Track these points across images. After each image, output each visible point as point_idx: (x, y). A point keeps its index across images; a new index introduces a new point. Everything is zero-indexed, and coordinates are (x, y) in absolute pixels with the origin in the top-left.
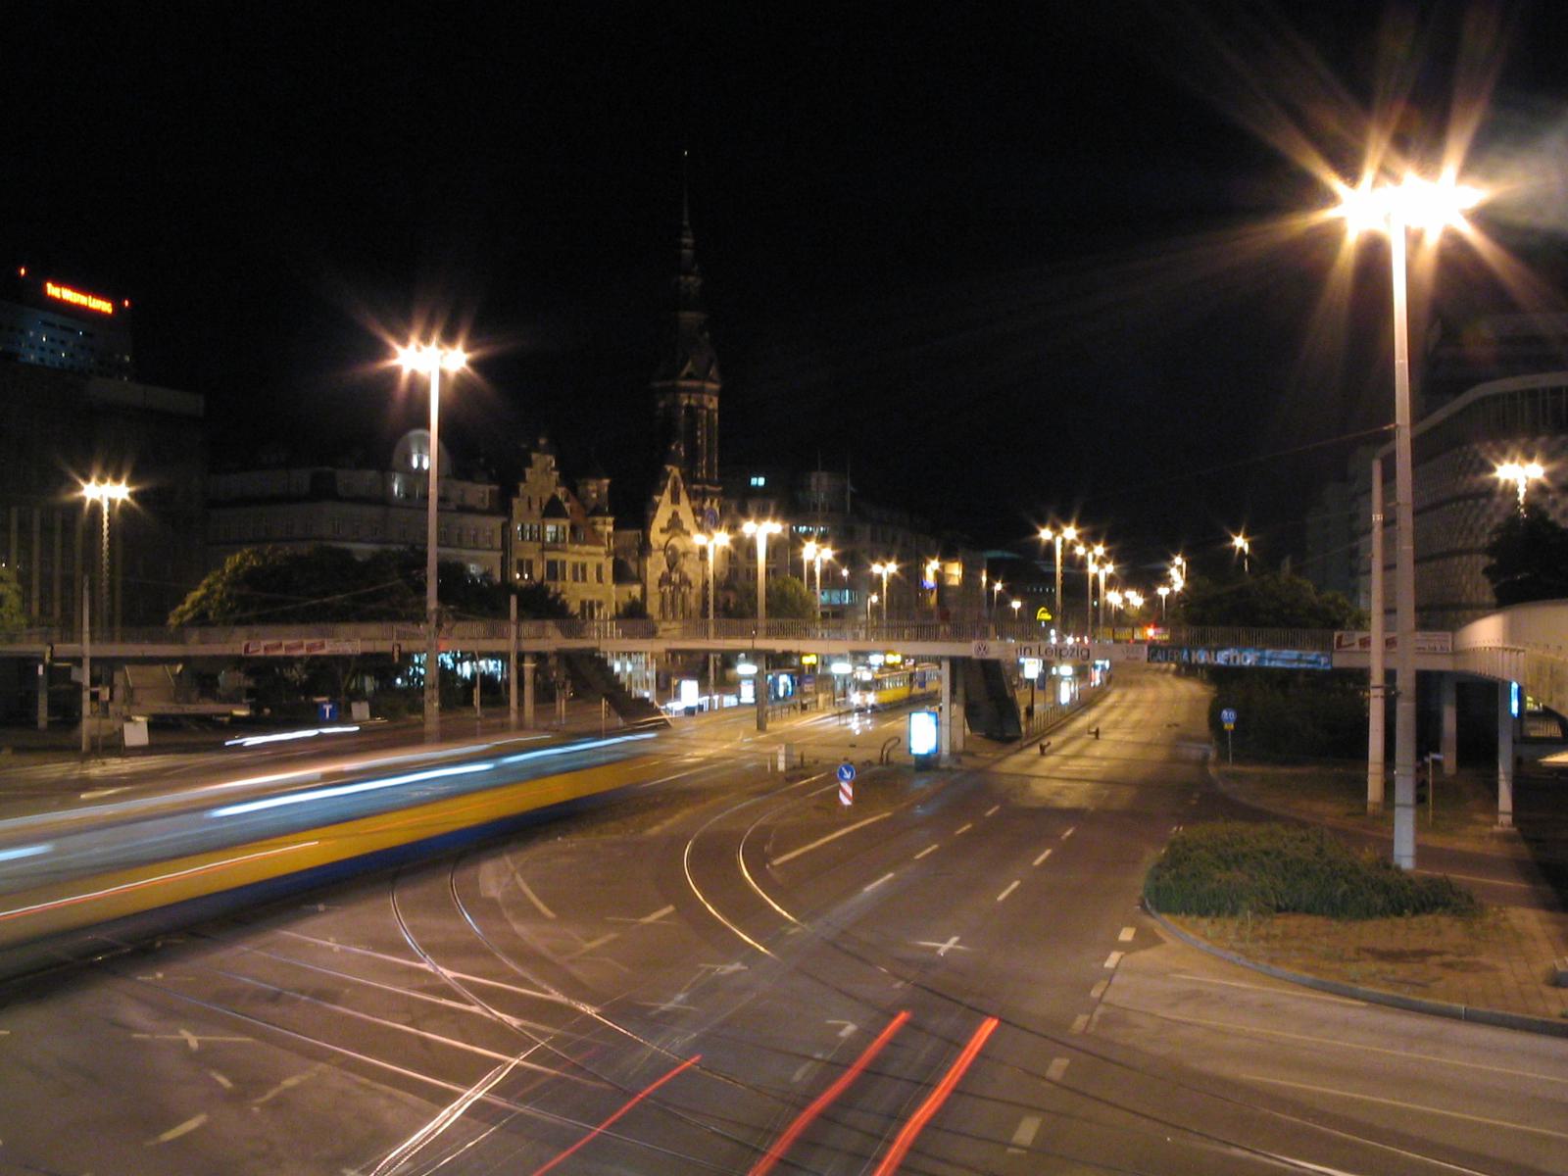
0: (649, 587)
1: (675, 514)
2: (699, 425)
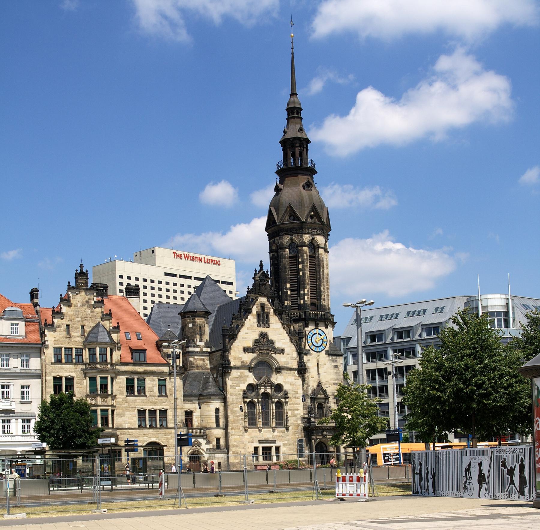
0: (230, 399)
1: (264, 336)
2: (300, 260)
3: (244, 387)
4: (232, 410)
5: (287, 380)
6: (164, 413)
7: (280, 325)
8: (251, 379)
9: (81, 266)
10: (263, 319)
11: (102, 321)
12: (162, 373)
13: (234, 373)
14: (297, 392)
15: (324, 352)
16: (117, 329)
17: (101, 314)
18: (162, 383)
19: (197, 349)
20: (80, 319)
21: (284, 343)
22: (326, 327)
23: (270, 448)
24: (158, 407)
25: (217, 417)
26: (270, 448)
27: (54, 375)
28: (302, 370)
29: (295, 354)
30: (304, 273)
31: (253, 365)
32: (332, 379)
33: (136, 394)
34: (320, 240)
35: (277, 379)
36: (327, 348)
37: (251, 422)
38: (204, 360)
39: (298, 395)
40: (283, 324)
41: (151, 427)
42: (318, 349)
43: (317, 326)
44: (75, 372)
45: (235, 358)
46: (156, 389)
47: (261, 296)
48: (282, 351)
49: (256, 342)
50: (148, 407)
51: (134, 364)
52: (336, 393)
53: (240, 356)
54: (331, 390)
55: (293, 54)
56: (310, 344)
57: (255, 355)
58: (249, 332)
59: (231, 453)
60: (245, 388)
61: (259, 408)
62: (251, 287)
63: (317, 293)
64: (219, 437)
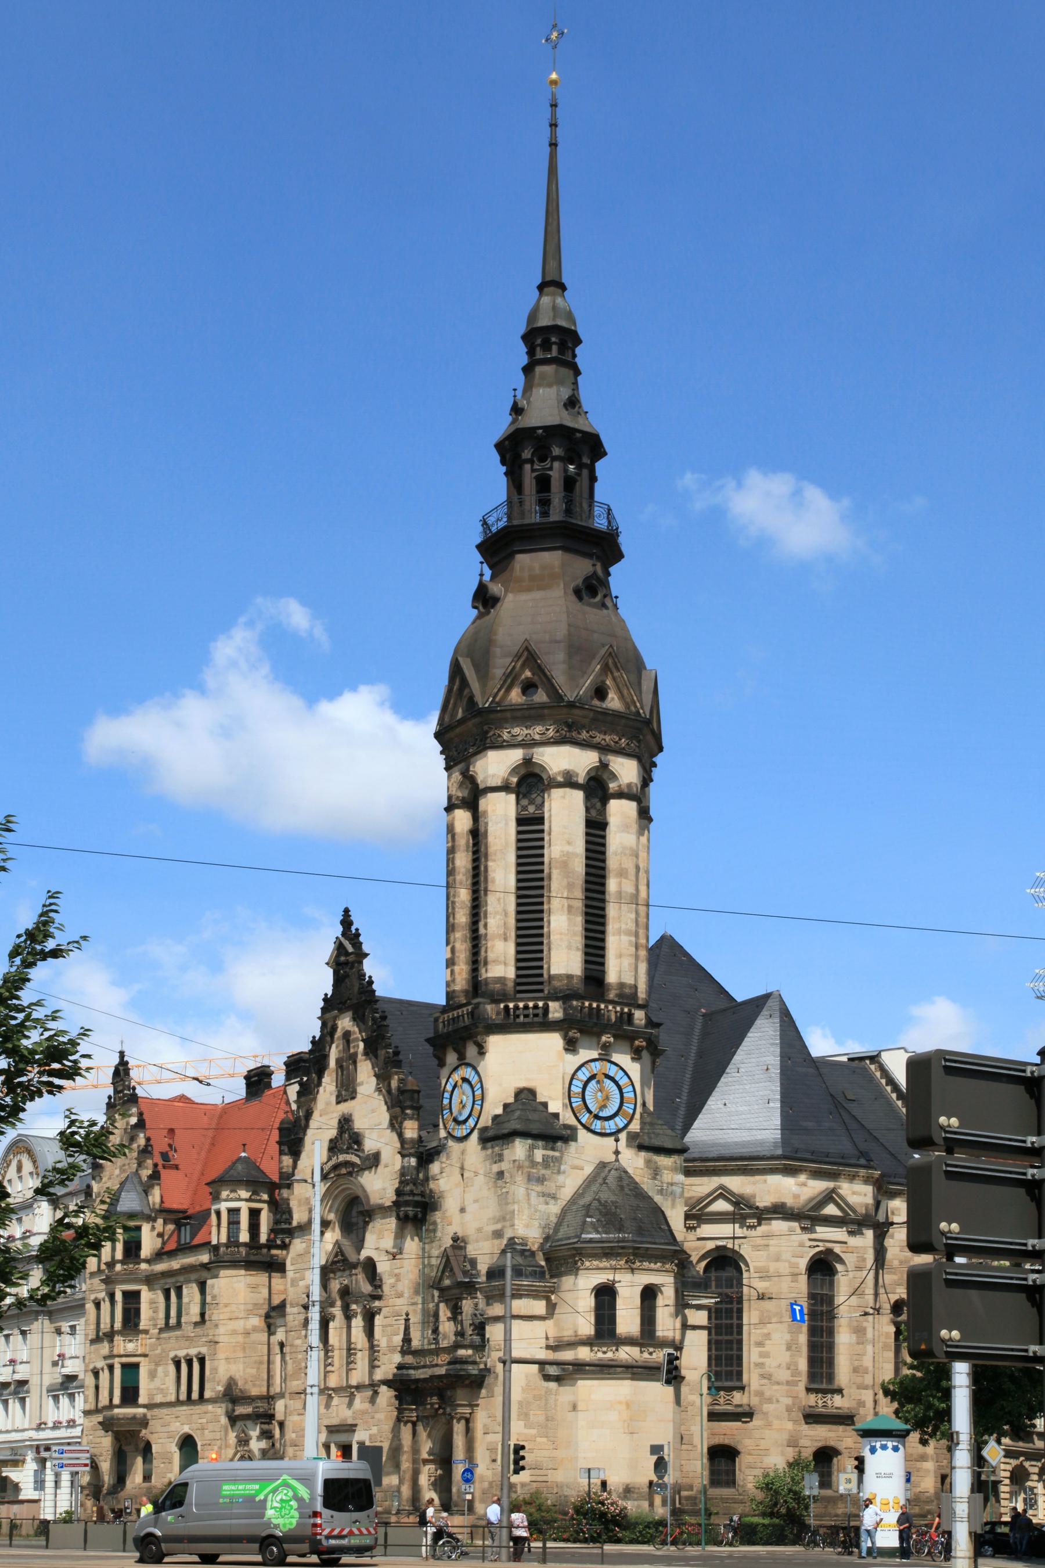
1: (345, 1123)
15: (475, 1135)
39: (400, 1287)
55: (553, 145)
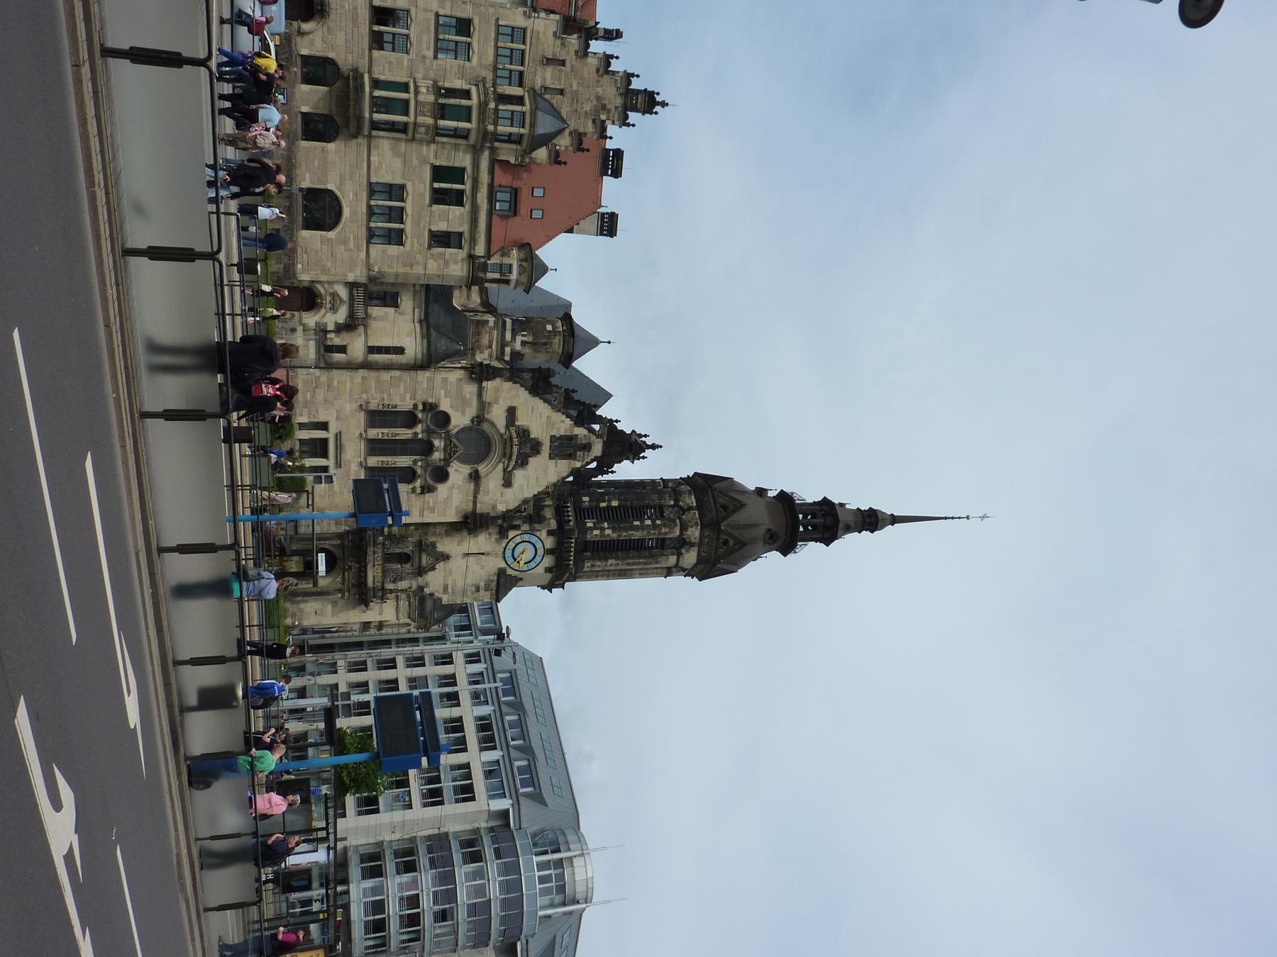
0: (423, 376)
1: (536, 448)
2: (658, 522)
3: (445, 406)
4: (400, 379)
5: (455, 492)
6: (396, 238)
7: (553, 478)
8: (459, 420)
9: (664, 104)
10: (564, 447)
11: (571, 133)
12: (473, 241)
13: (470, 389)
14: (432, 510)
15: (503, 565)
16: (556, 158)
17: (581, 130)
18: (454, 240)
19: (508, 336)
20: (575, 88)
21: (521, 487)
22: (548, 570)
23: (325, 455)
24: (408, 226)
25: (387, 350)
26: (325, 455)
27: (476, 21)
28: (472, 523)
29: (502, 508)
30: (637, 528)
31: (486, 426)
32: (454, 581)
33: (436, 185)
34: (690, 558)
35: (459, 472)
36: (509, 572)
37: (377, 417)
38: (490, 347)
39: (426, 513)
40: (555, 485)
41: (371, 212)
42: (508, 553)
43: (548, 552)
44: (480, 65)
45: (497, 390)
46: (442, 226)
47: (605, 444)
48: (508, 483)
49: (524, 433)
50: (409, 206)
51: (491, 186)
52: (427, 591)
53: (501, 401)
54: (434, 581)
56: (518, 539)
57: (502, 430)
58: (542, 419)
59: (317, 372)
60: (442, 408)
61: (405, 433)
62: (619, 426)
63: (605, 549)
64: (349, 350)
